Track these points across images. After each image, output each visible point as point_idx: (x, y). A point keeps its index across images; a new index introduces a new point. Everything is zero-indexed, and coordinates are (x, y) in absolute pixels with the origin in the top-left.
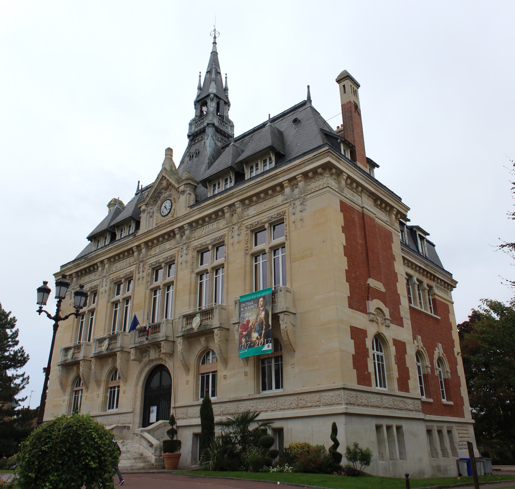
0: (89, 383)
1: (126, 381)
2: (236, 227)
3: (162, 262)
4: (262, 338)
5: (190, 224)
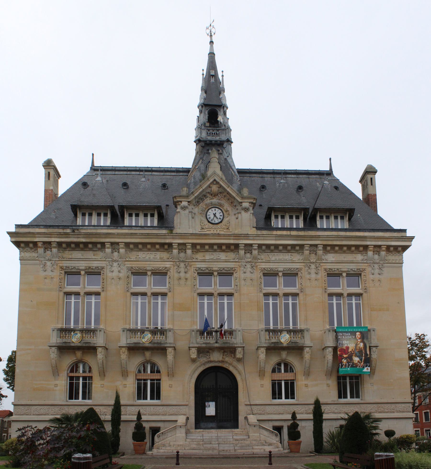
1: (173, 376)
2: (313, 266)
3: (216, 271)
4: (363, 363)
5: (260, 246)
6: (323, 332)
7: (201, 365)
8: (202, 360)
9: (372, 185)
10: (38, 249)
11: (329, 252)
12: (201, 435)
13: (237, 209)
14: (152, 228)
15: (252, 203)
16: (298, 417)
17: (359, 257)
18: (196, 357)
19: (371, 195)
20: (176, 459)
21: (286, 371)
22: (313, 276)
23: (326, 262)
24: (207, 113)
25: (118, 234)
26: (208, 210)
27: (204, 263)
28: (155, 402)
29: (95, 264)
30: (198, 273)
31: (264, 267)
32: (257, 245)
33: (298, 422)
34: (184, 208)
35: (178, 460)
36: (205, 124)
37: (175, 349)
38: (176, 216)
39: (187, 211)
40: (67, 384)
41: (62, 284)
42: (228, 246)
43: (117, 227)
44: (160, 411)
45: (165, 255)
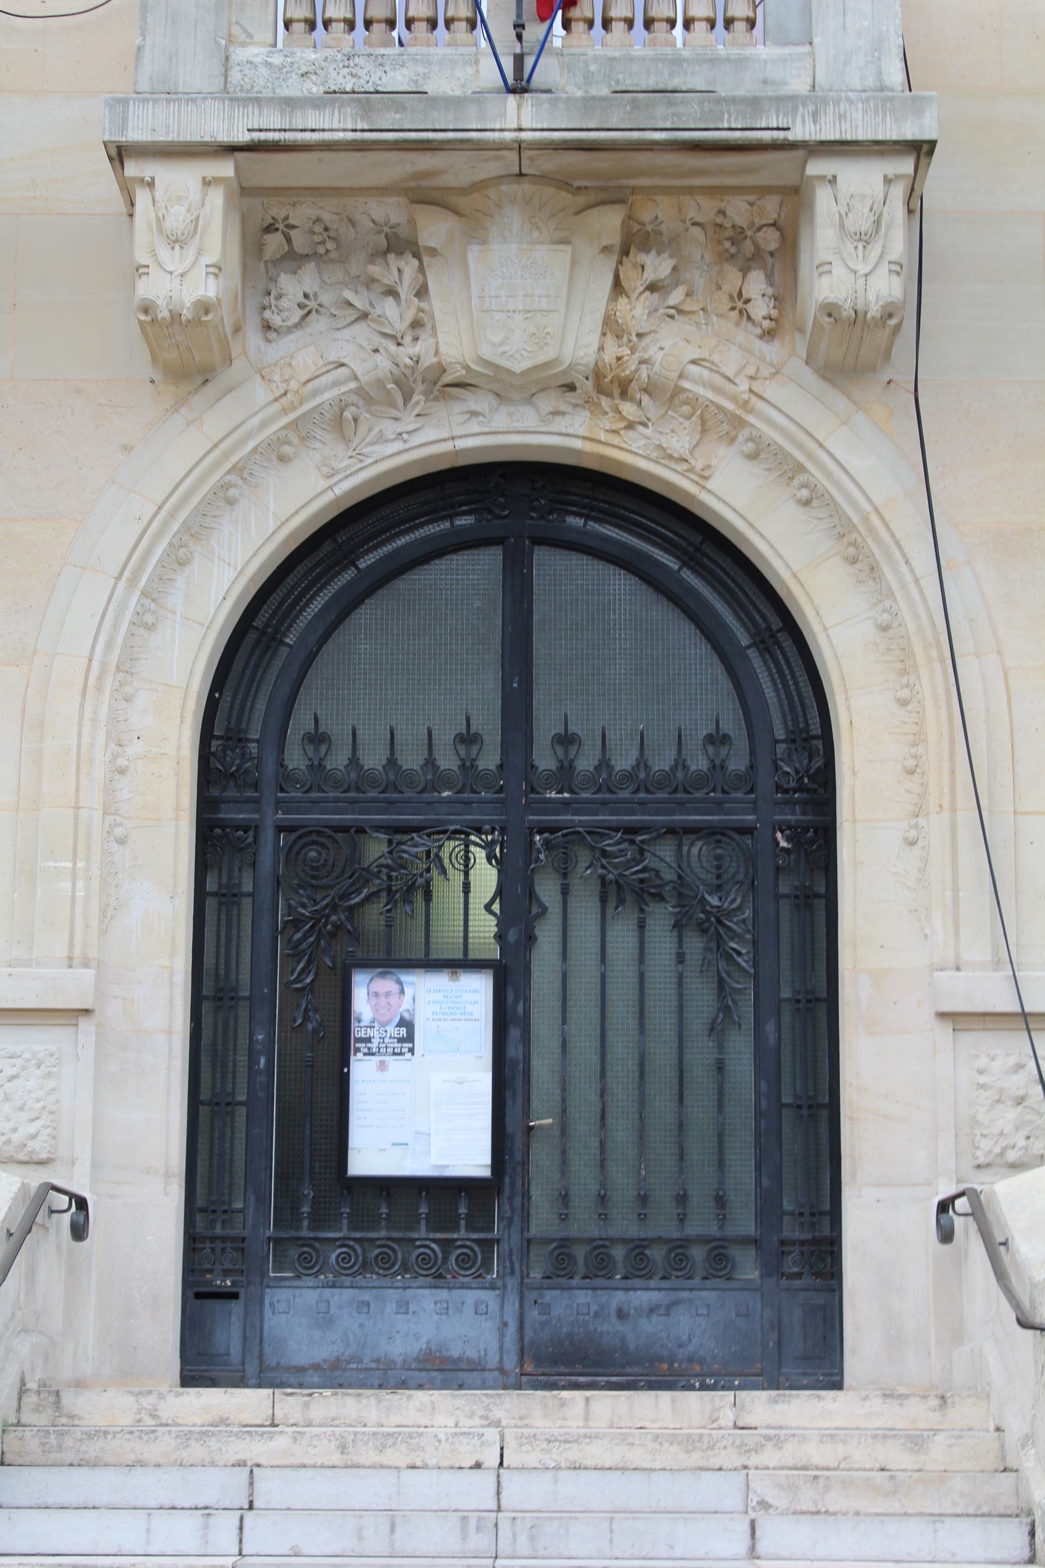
7: (302, 430)
18: (210, 289)
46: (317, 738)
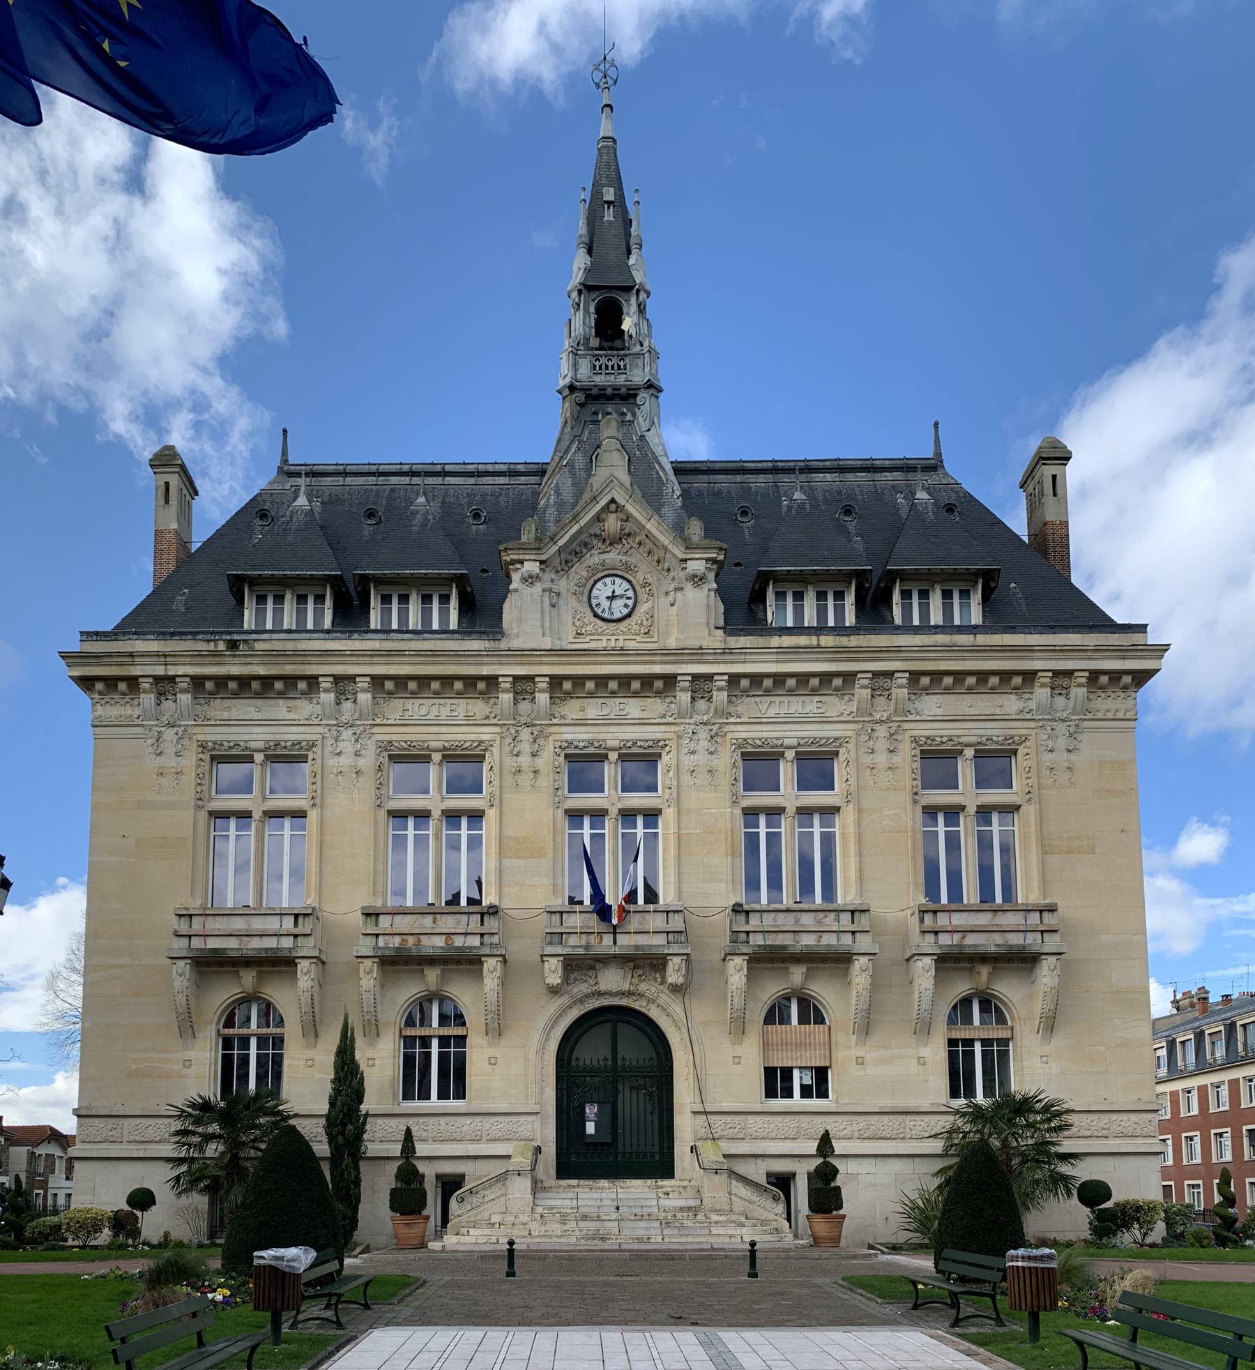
0: (321, 1023)
2: (882, 731)
5: (734, 679)
6: (909, 912)
7: (574, 1003)
8: (575, 990)
9: (1055, 495)
10: (142, 696)
11: (925, 690)
12: (571, 1195)
13: (673, 579)
14: (443, 636)
15: (714, 561)
16: (839, 1147)
17: (1011, 704)
18: (559, 981)
19: (1053, 523)
20: (506, 1262)
21: (803, 1020)
22: (882, 759)
23: (918, 718)
24: (592, 309)
25: (354, 654)
26: (596, 582)
27: (583, 729)
28: (452, 1104)
29: (291, 735)
30: (566, 756)
31: (744, 735)
32: (726, 677)
33: (835, 1162)
34: (530, 579)
35: (511, 1263)
36: (587, 339)
37: (505, 961)
38: (508, 601)
39: (538, 587)
40: (216, 1059)
41: (205, 788)
42: (647, 681)
43: (352, 632)
44: (465, 1129)
45: (478, 707)
46: (577, 1059)
